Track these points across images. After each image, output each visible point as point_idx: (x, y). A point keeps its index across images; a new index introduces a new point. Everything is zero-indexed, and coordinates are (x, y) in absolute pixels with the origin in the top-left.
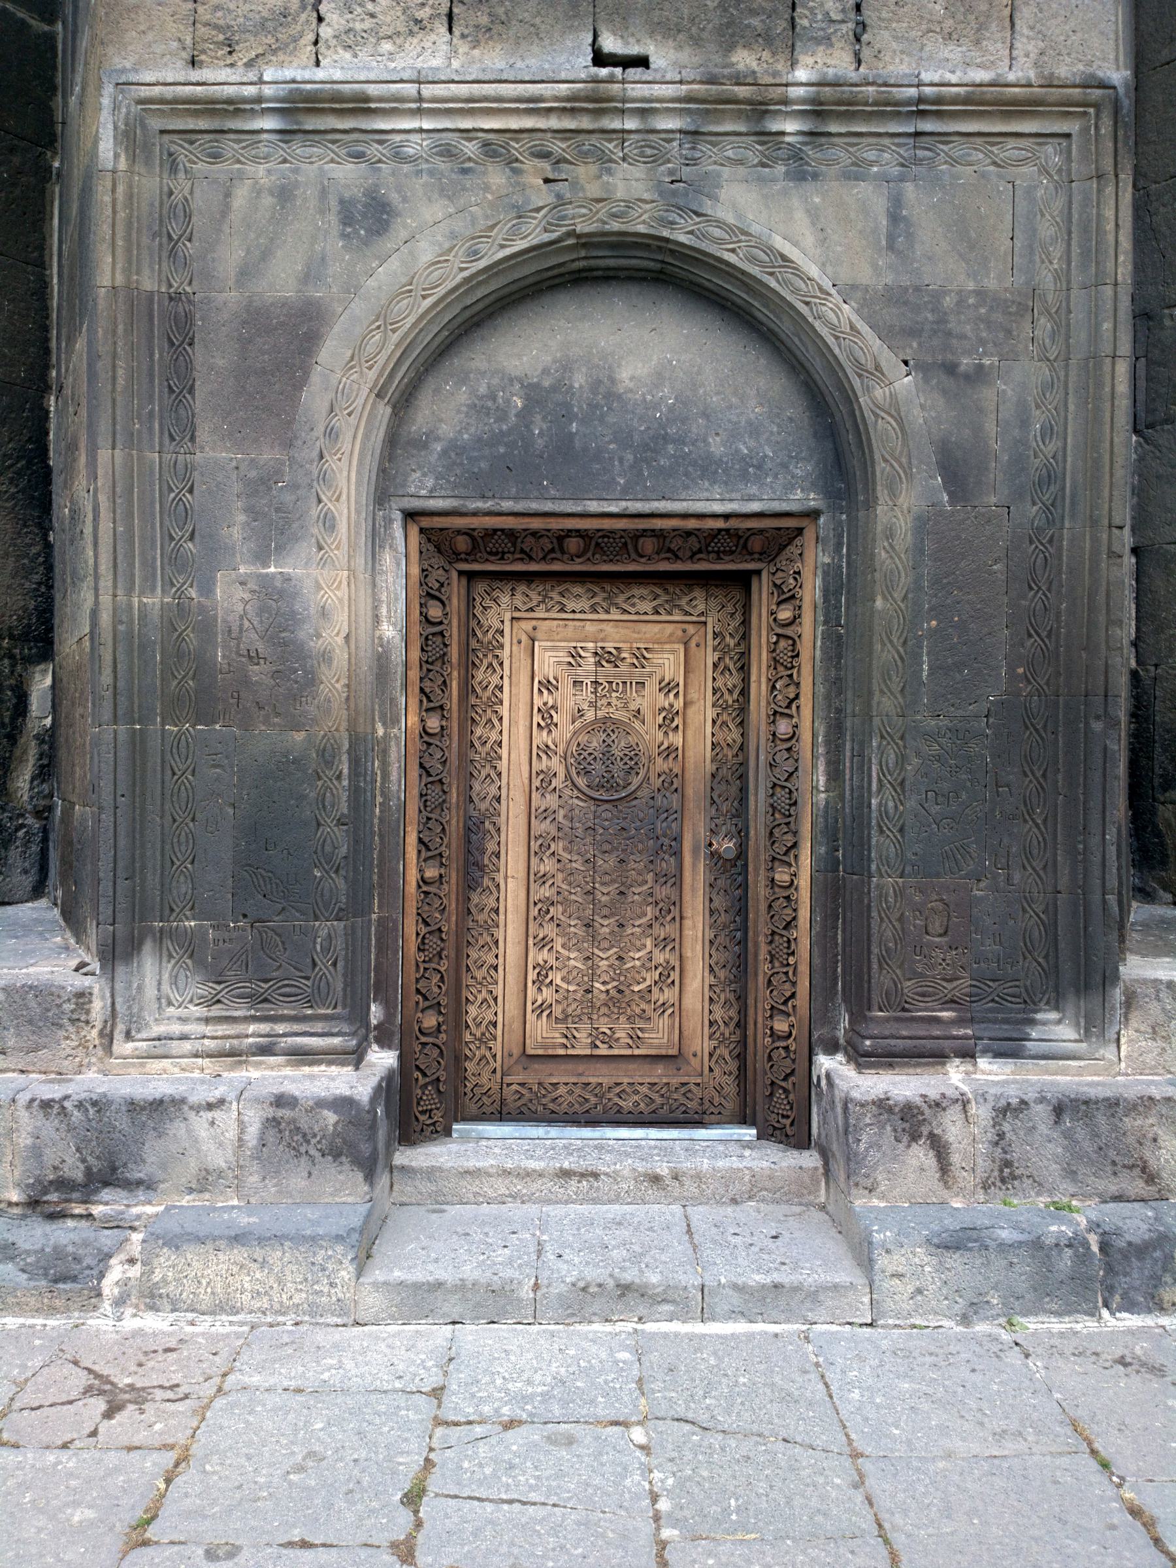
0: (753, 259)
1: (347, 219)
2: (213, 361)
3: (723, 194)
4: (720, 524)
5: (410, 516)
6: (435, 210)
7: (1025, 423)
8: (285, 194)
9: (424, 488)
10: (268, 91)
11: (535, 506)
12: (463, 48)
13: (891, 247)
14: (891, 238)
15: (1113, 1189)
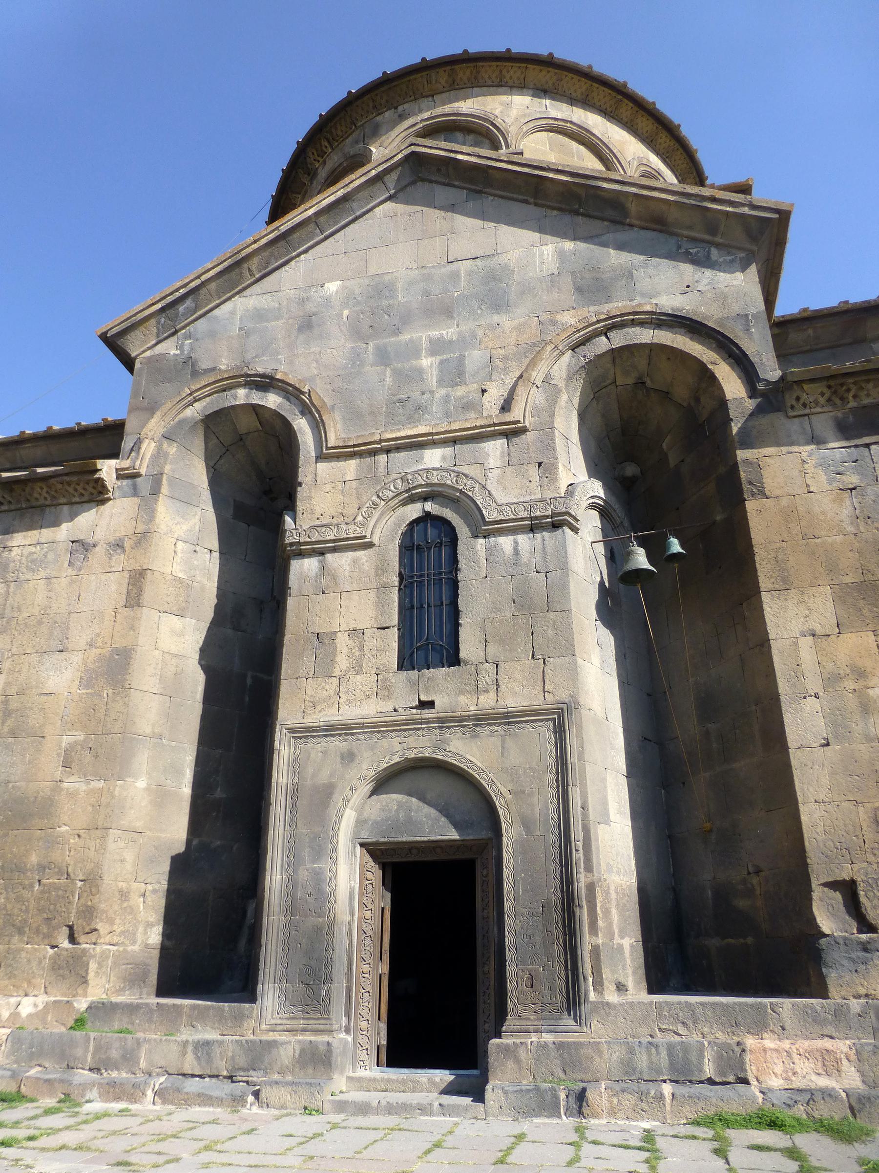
0: (461, 762)
1: (342, 758)
2: (303, 803)
3: (452, 744)
4: (460, 843)
5: (362, 845)
6: (367, 754)
7: (547, 808)
8: (325, 753)
9: (367, 836)
10: (321, 724)
11: (400, 839)
12: (380, 702)
13: (503, 756)
14: (502, 753)
15: (579, 1077)
